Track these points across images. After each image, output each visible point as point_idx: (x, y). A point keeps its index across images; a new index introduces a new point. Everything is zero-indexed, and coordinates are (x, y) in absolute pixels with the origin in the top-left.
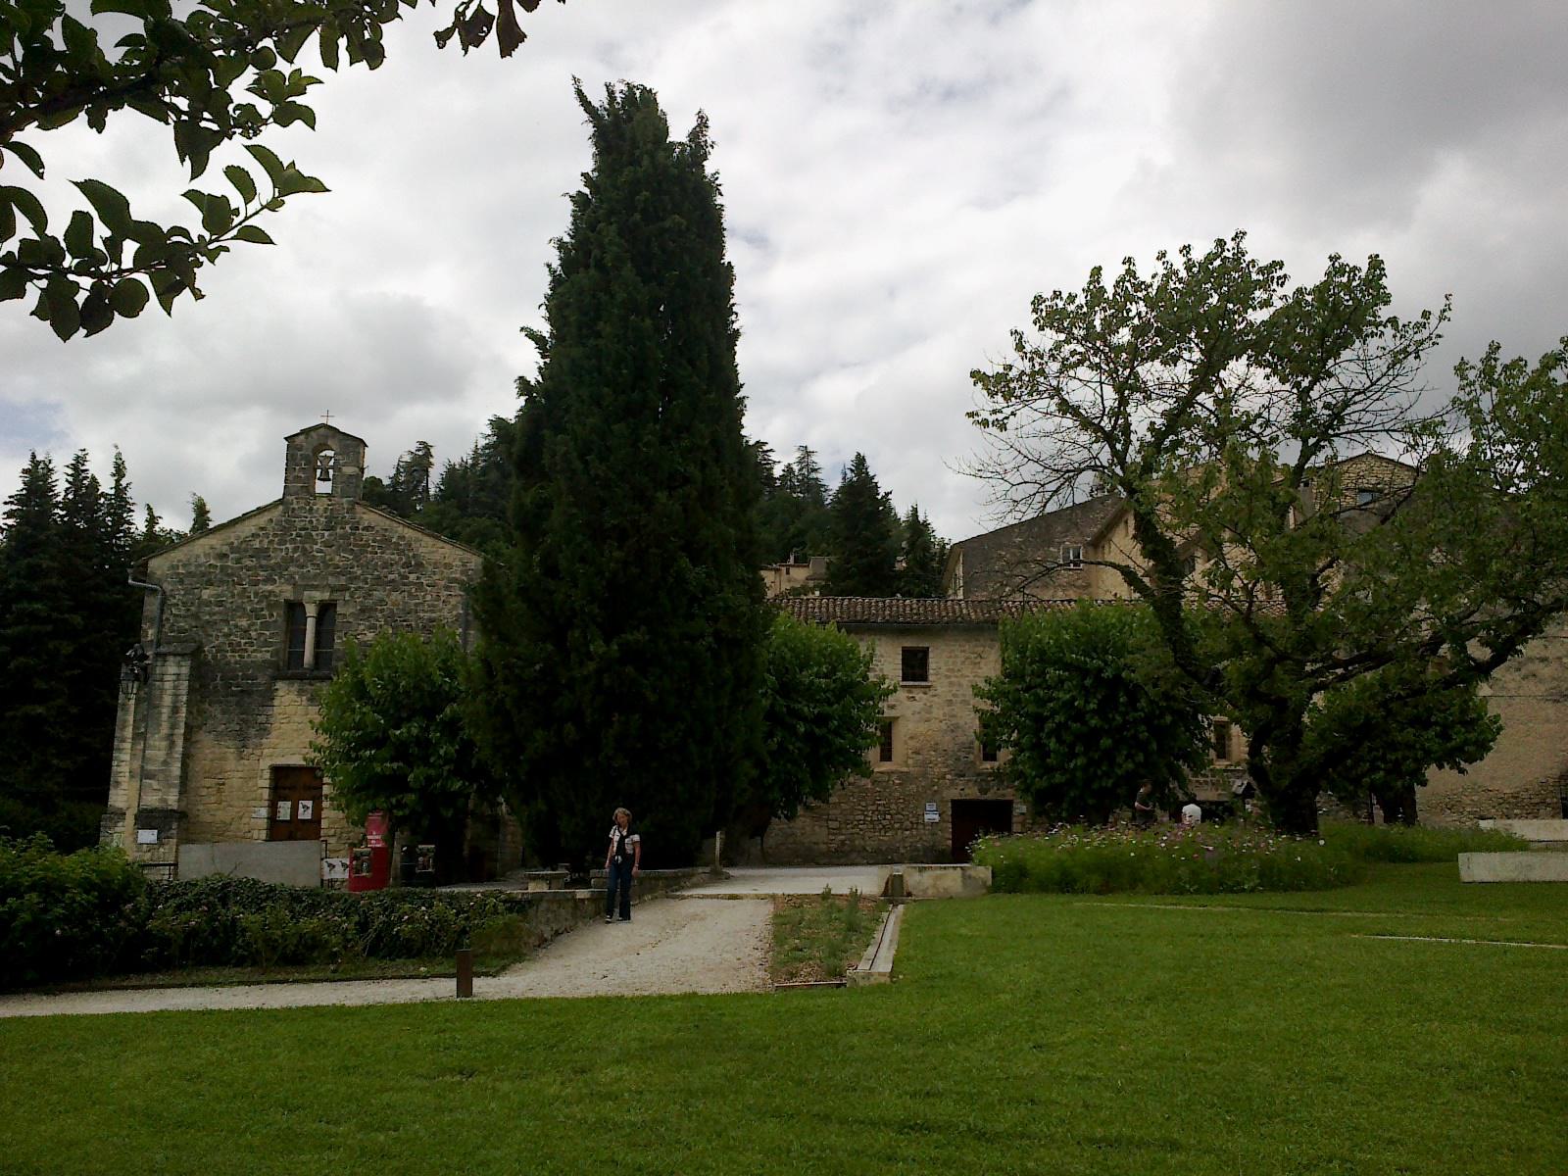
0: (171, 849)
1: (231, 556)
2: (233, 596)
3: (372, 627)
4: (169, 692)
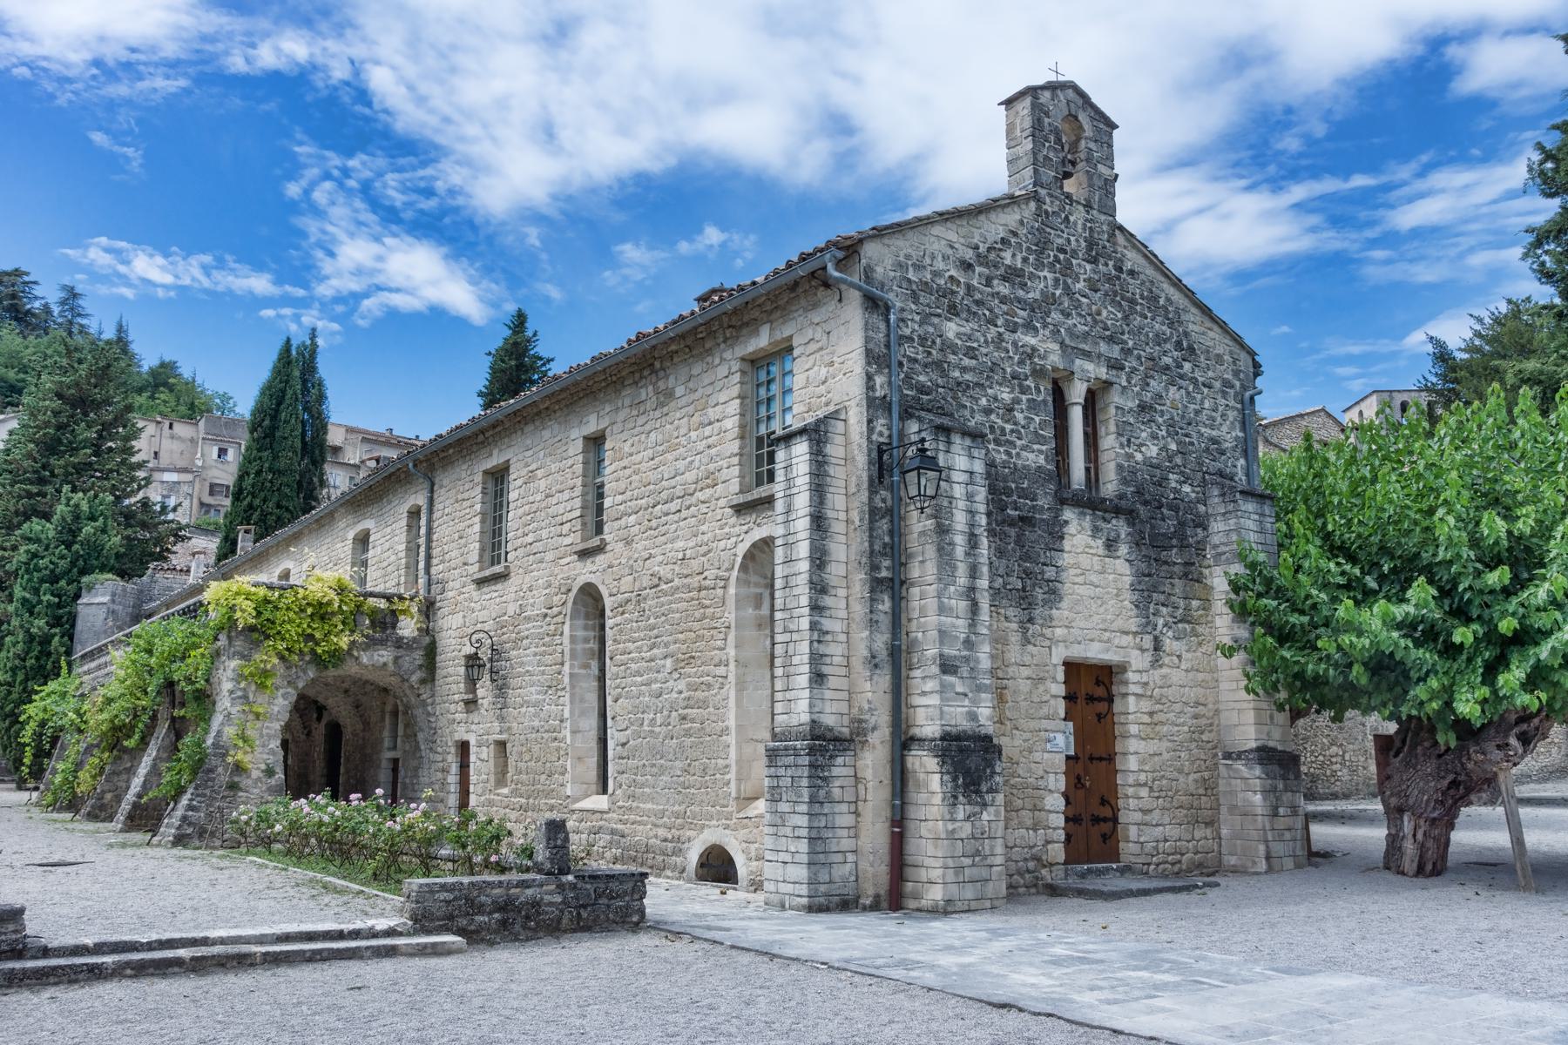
0: (997, 813)
1: (978, 269)
2: (986, 341)
3: (1154, 437)
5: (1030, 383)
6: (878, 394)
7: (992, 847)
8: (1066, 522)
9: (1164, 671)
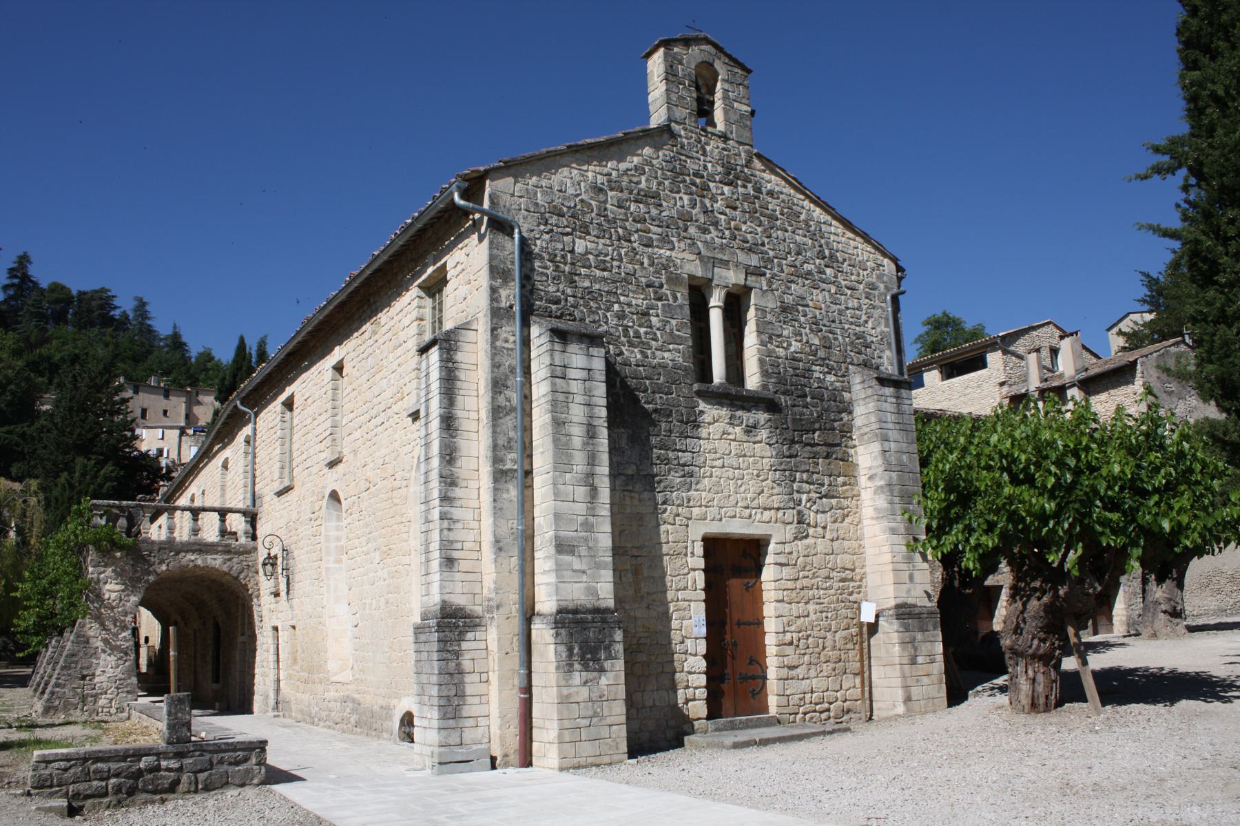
0: (616, 677)
1: (610, 194)
5: (665, 290)
6: (503, 305)
8: (702, 412)
9: (810, 541)
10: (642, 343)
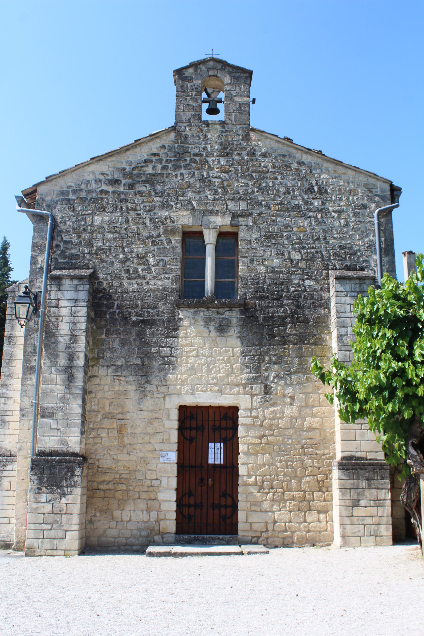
4: (66, 319)
7: (69, 519)
8: (181, 319)
10: (139, 277)
